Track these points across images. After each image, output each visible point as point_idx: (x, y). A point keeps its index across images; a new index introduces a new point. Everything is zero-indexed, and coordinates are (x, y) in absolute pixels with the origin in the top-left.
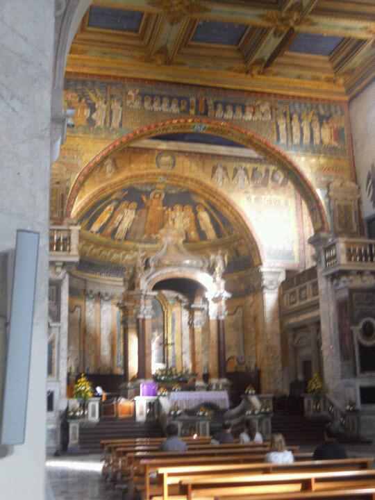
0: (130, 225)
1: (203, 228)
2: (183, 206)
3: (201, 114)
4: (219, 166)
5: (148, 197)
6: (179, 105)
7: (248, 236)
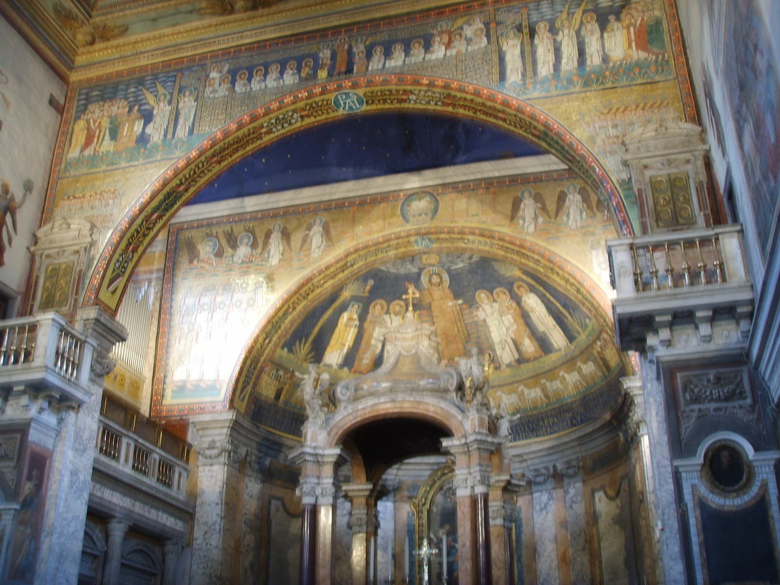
1: (541, 328)
3: (339, 74)
4: (526, 194)
6: (299, 69)
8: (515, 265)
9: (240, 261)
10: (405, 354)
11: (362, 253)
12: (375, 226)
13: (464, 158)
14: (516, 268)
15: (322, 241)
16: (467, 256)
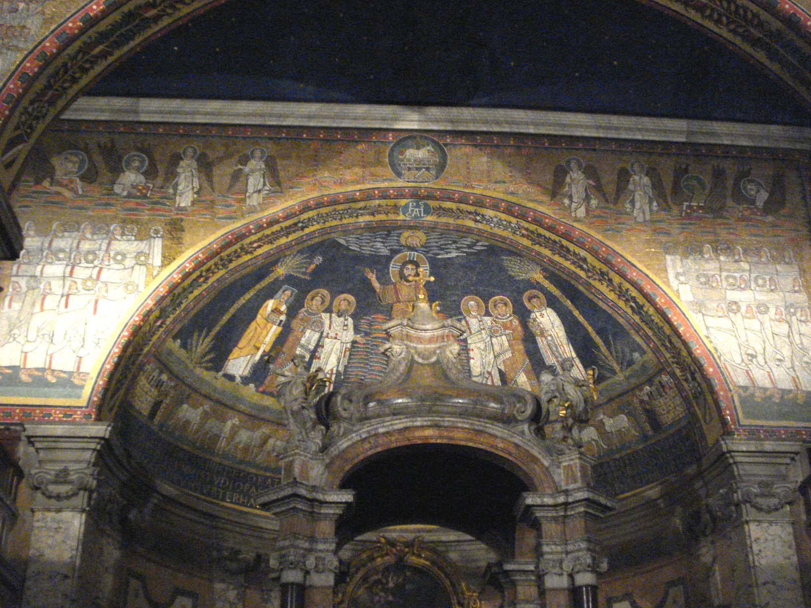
0: (345, 361)
2: (486, 299)
4: (573, 164)
5: (383, 278)
7: (677, 354)
8: (538, 264)
9: (125, 193)
10: (420, 361)
11: (324, 210)
12: (348, 175)
13: (485, 100)
14: (539, 269)
15: (264, 185)
16: (469, 241)
